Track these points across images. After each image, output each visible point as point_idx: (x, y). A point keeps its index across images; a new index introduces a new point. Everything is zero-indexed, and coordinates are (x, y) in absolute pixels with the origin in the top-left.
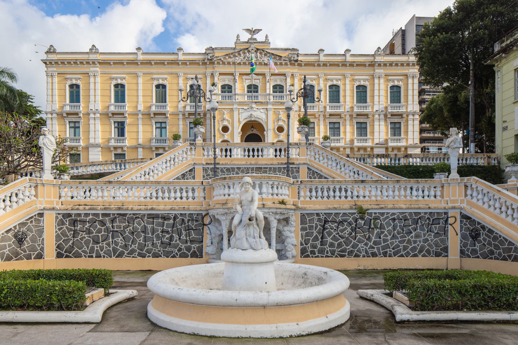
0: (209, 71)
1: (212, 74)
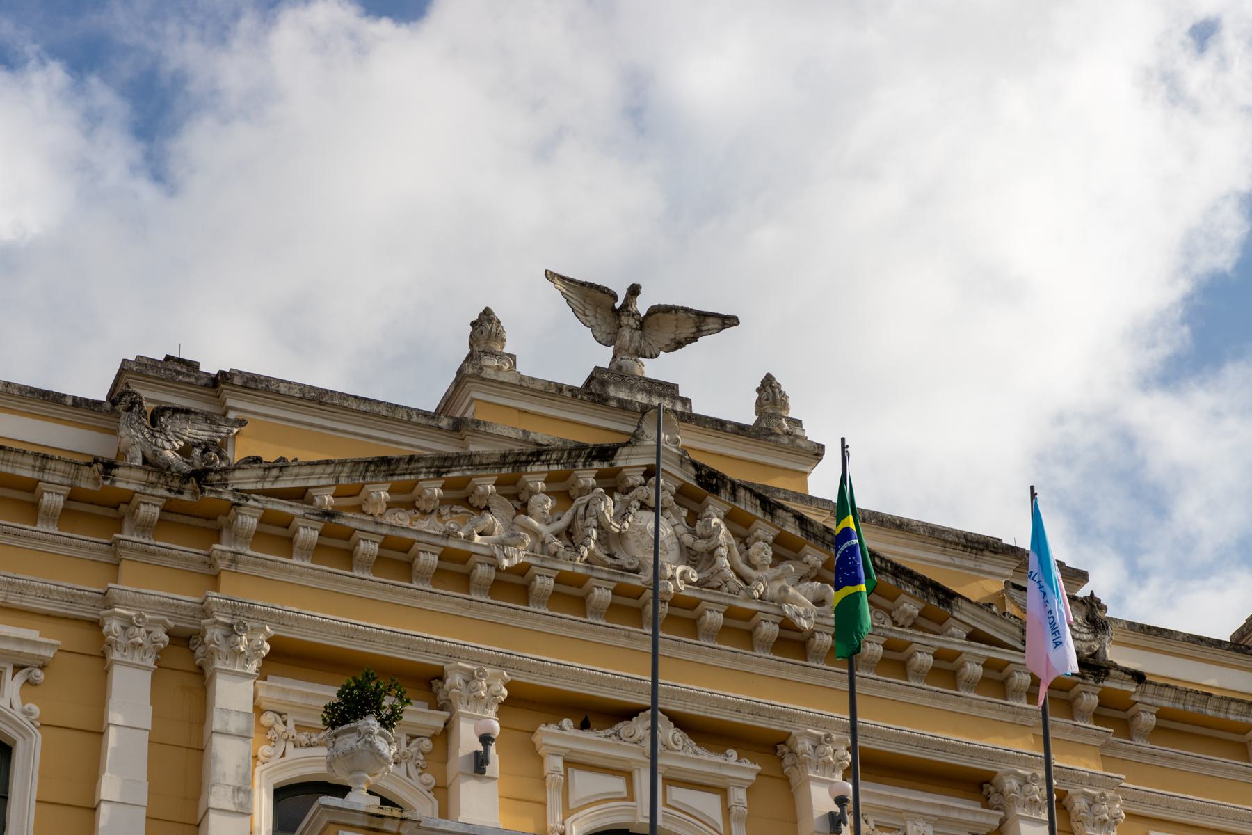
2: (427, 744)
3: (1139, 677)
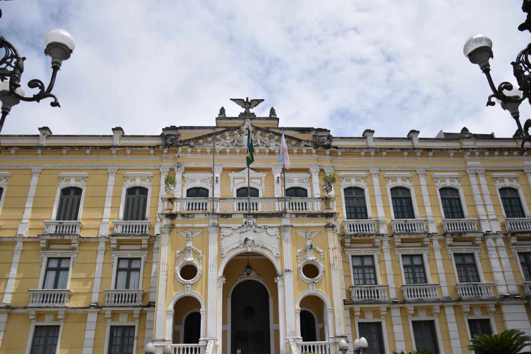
0: (167, 163)
2: (211, 179)
3: (337, 148)
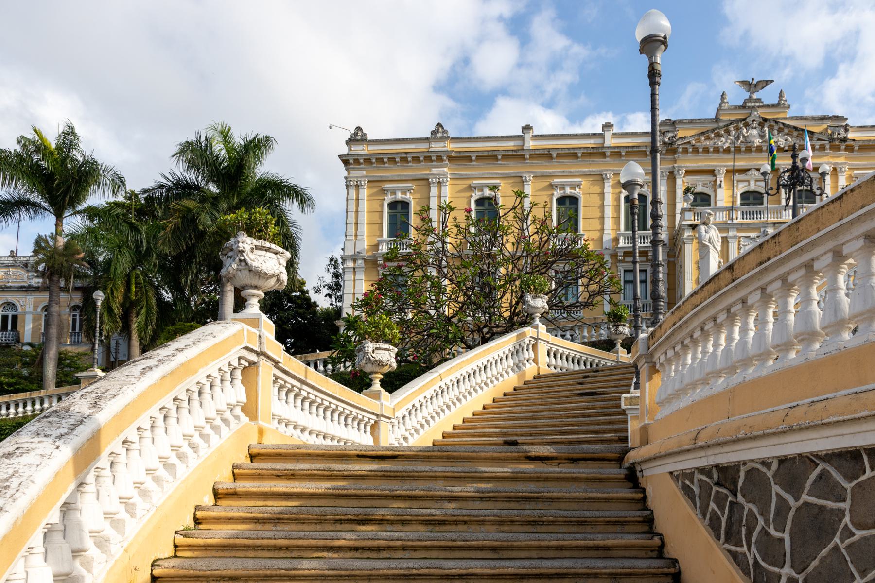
1: (671, 173)
